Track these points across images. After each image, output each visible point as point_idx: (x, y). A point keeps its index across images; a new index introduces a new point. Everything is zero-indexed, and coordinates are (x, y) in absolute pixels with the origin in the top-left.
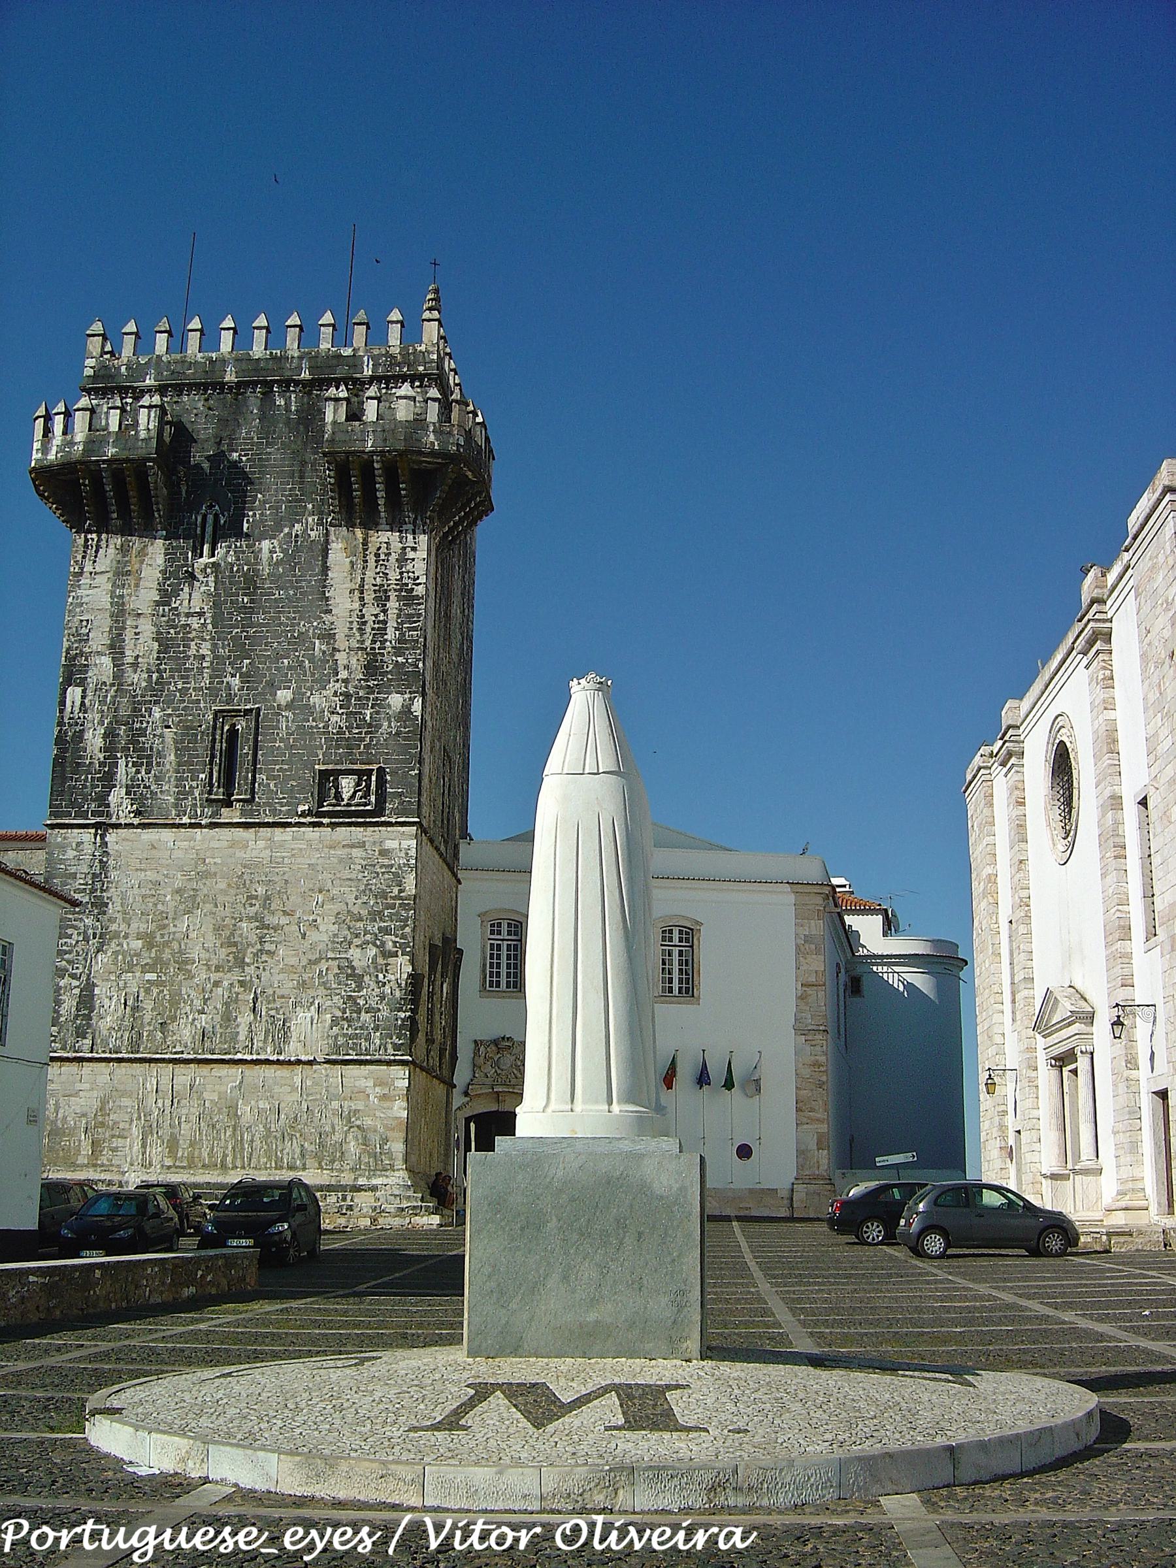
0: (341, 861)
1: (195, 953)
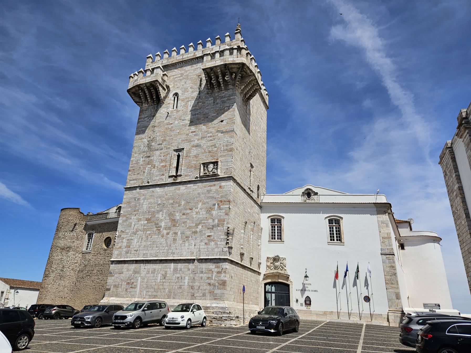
0: (207, 191)
1: (163, 224)
